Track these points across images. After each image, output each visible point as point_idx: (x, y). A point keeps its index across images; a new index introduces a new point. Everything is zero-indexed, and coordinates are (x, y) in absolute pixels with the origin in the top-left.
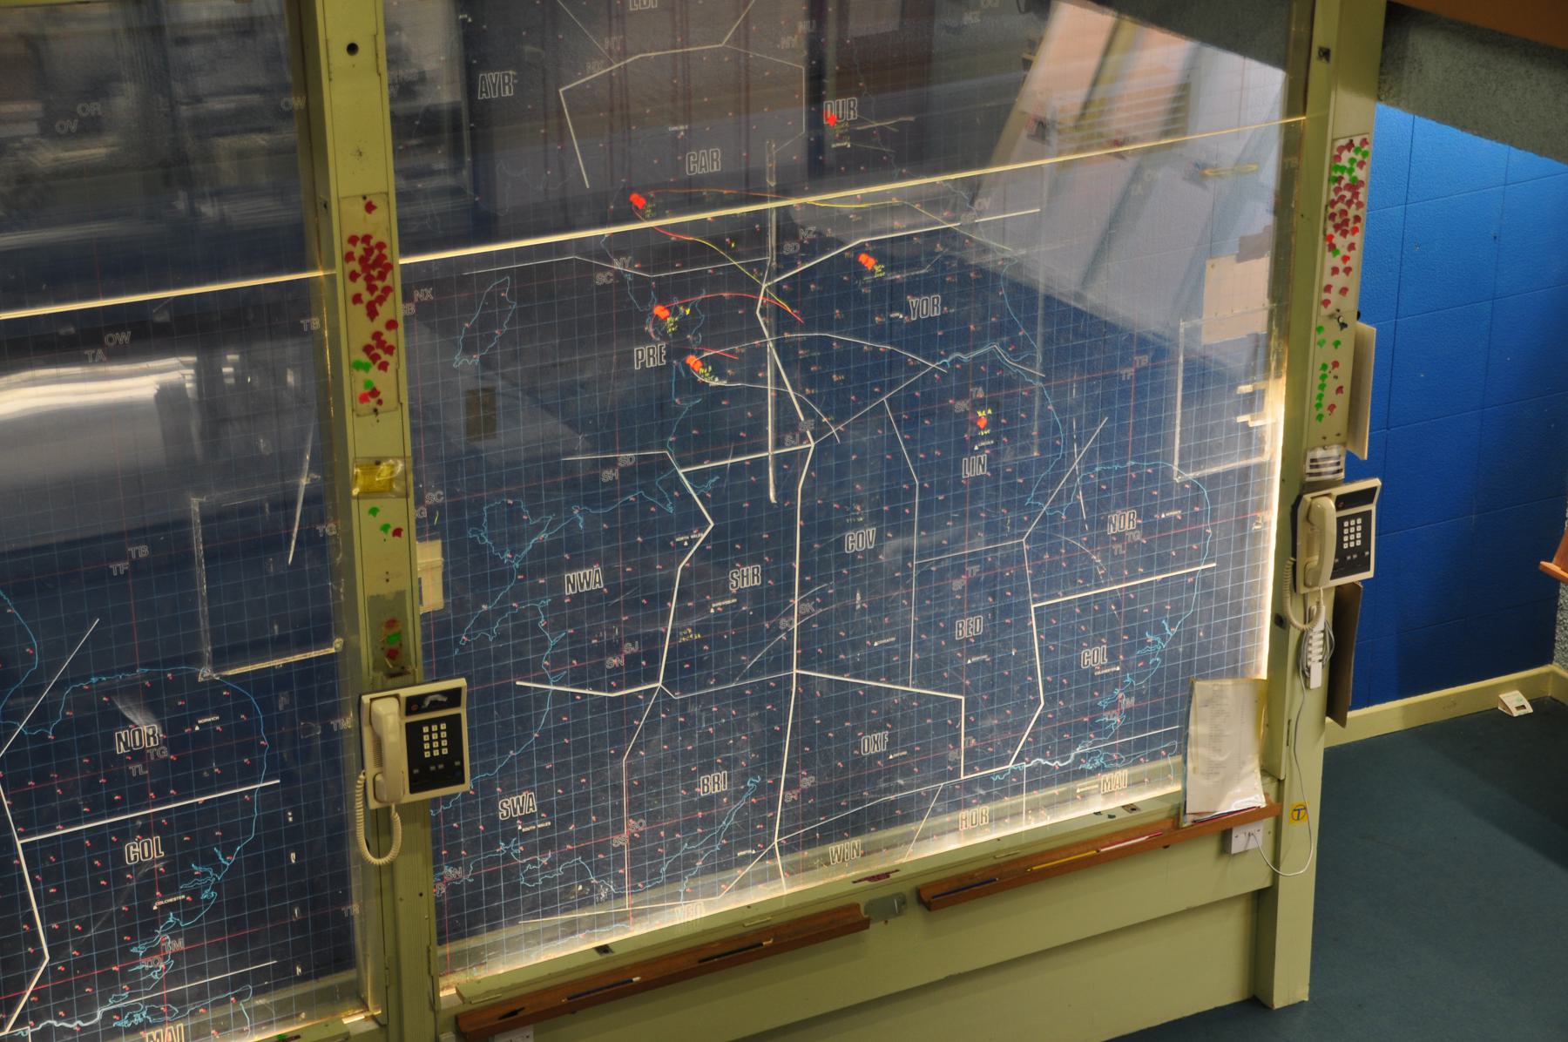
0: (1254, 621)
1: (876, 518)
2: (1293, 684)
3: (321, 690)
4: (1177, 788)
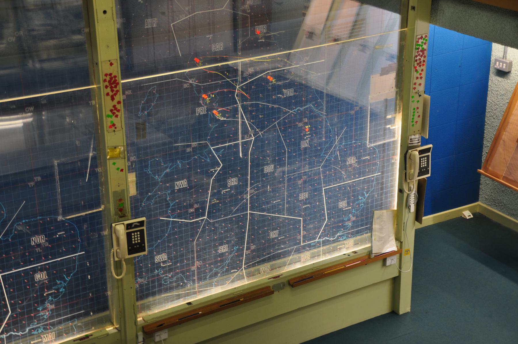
0: (392, 191)
1: (274, 161)
2: (405, 211)
3: (96, 222)
4: (369, 245)
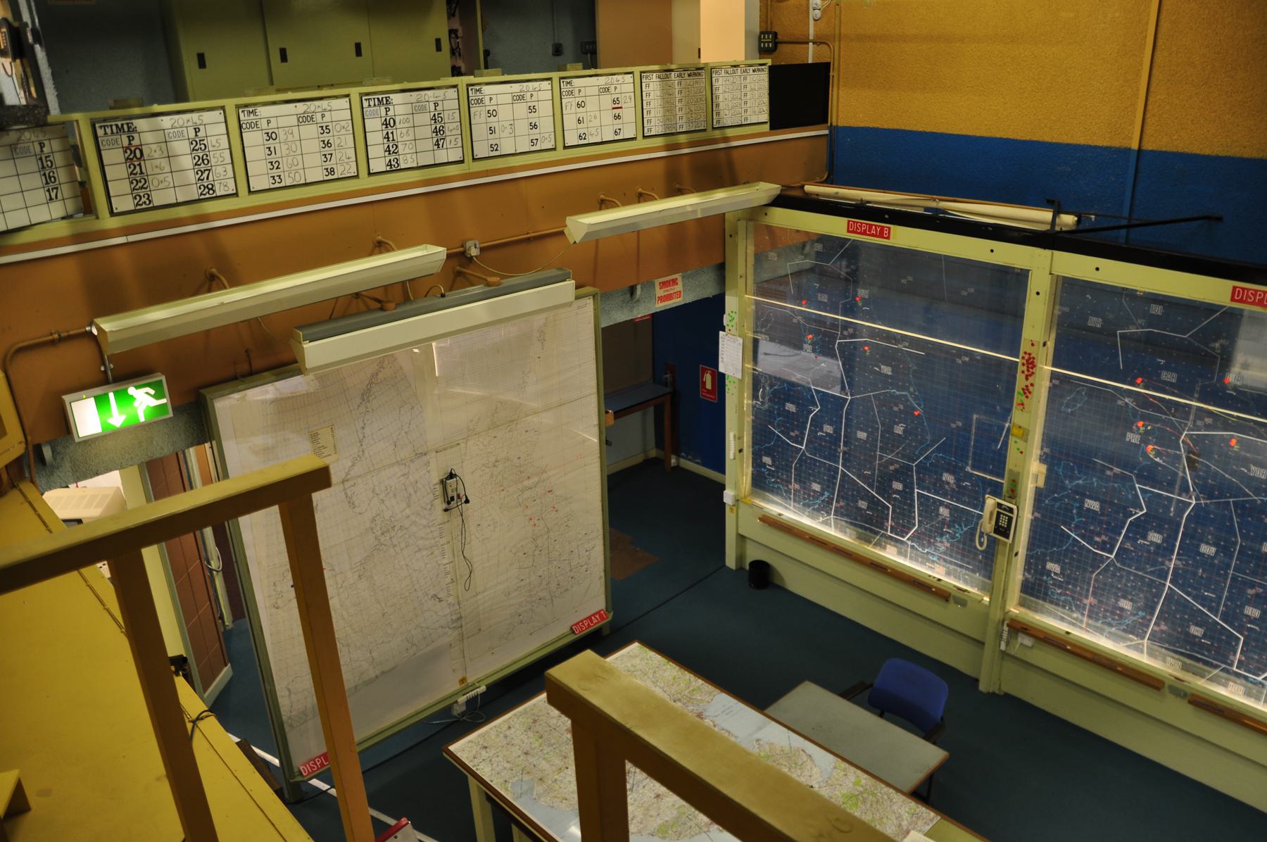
1: (1215, 544)
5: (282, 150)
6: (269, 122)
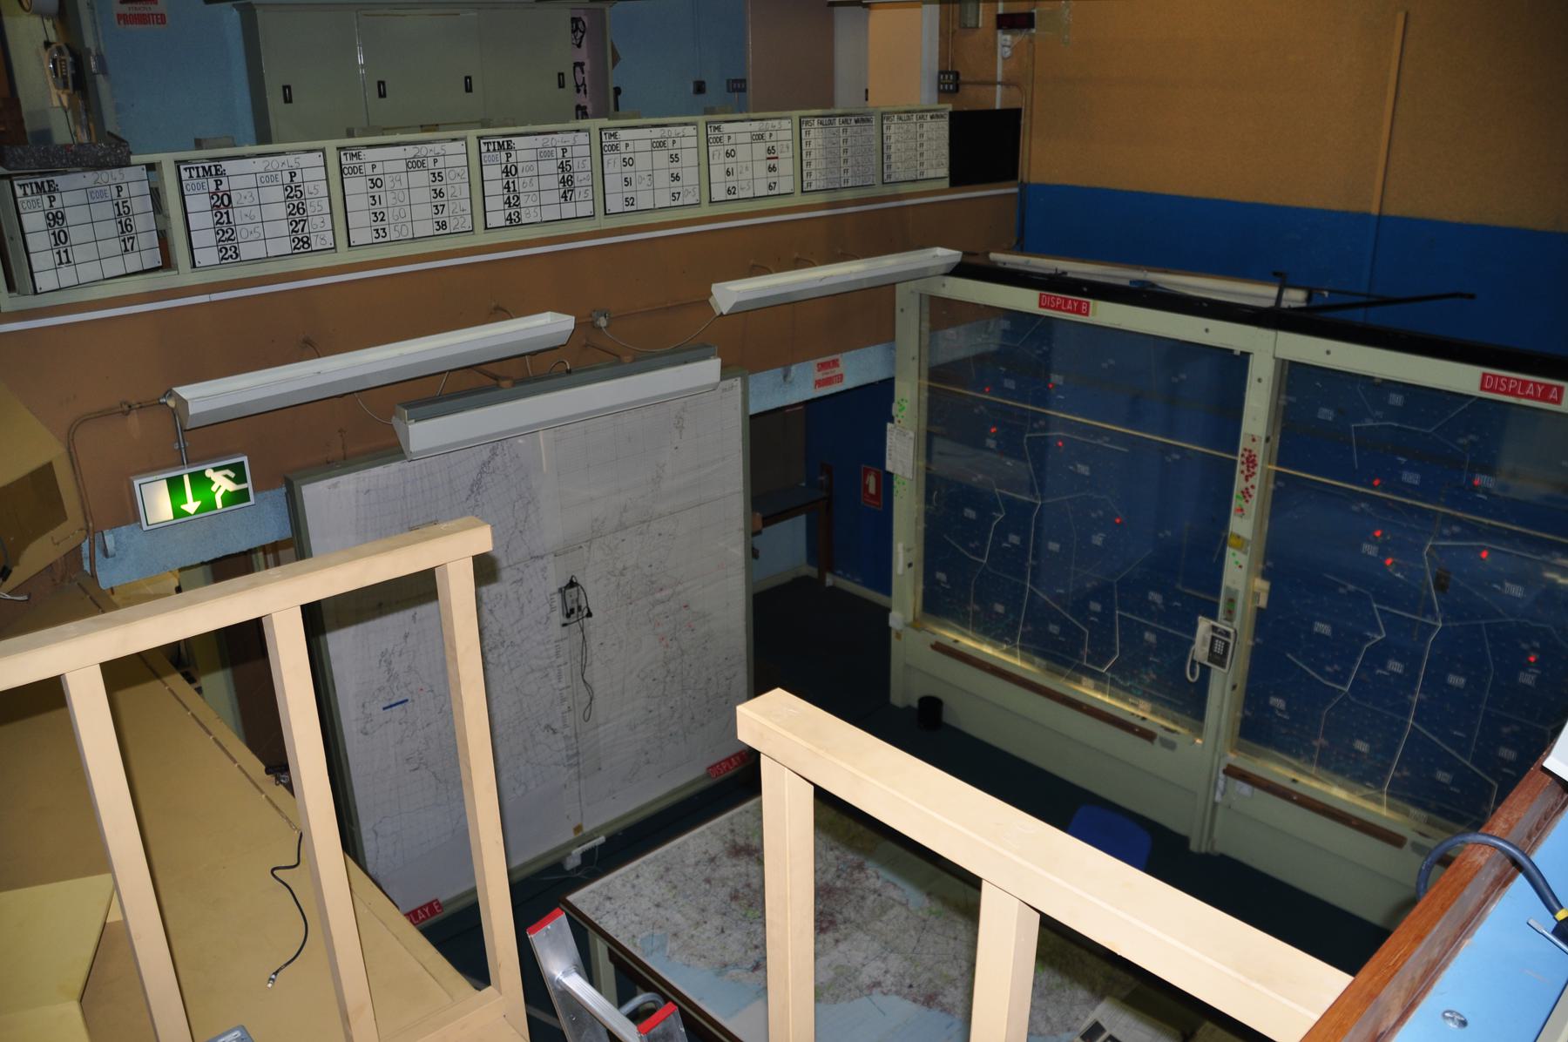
5: (388, 199)
6: (374, 167)
